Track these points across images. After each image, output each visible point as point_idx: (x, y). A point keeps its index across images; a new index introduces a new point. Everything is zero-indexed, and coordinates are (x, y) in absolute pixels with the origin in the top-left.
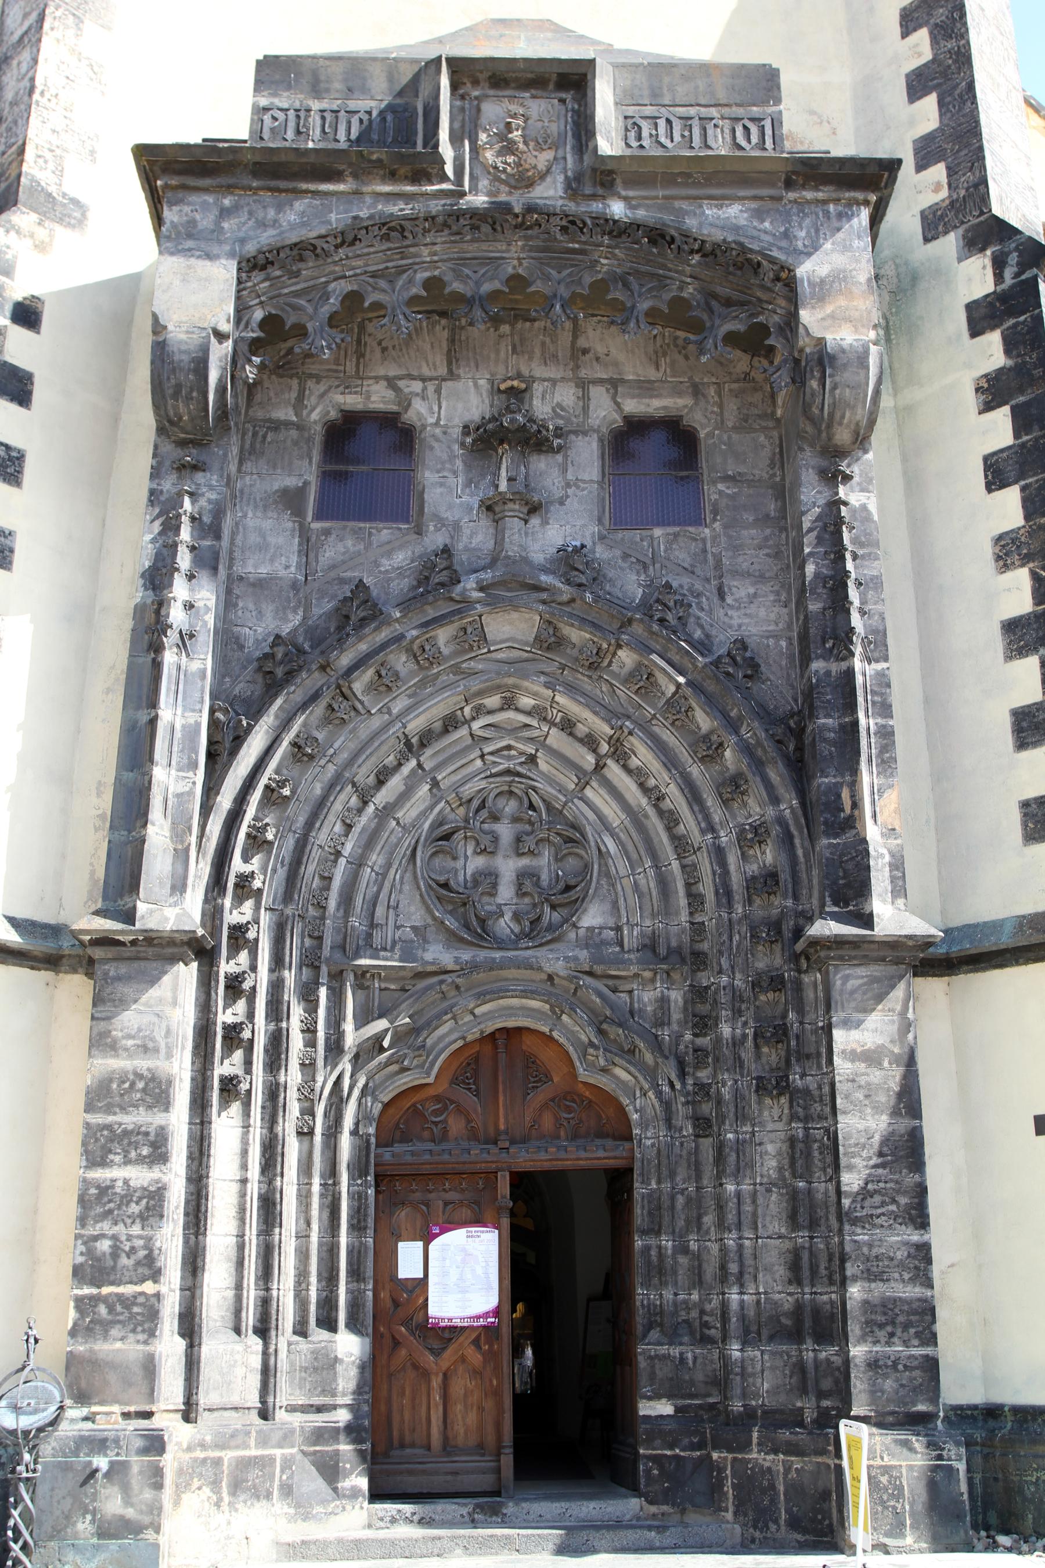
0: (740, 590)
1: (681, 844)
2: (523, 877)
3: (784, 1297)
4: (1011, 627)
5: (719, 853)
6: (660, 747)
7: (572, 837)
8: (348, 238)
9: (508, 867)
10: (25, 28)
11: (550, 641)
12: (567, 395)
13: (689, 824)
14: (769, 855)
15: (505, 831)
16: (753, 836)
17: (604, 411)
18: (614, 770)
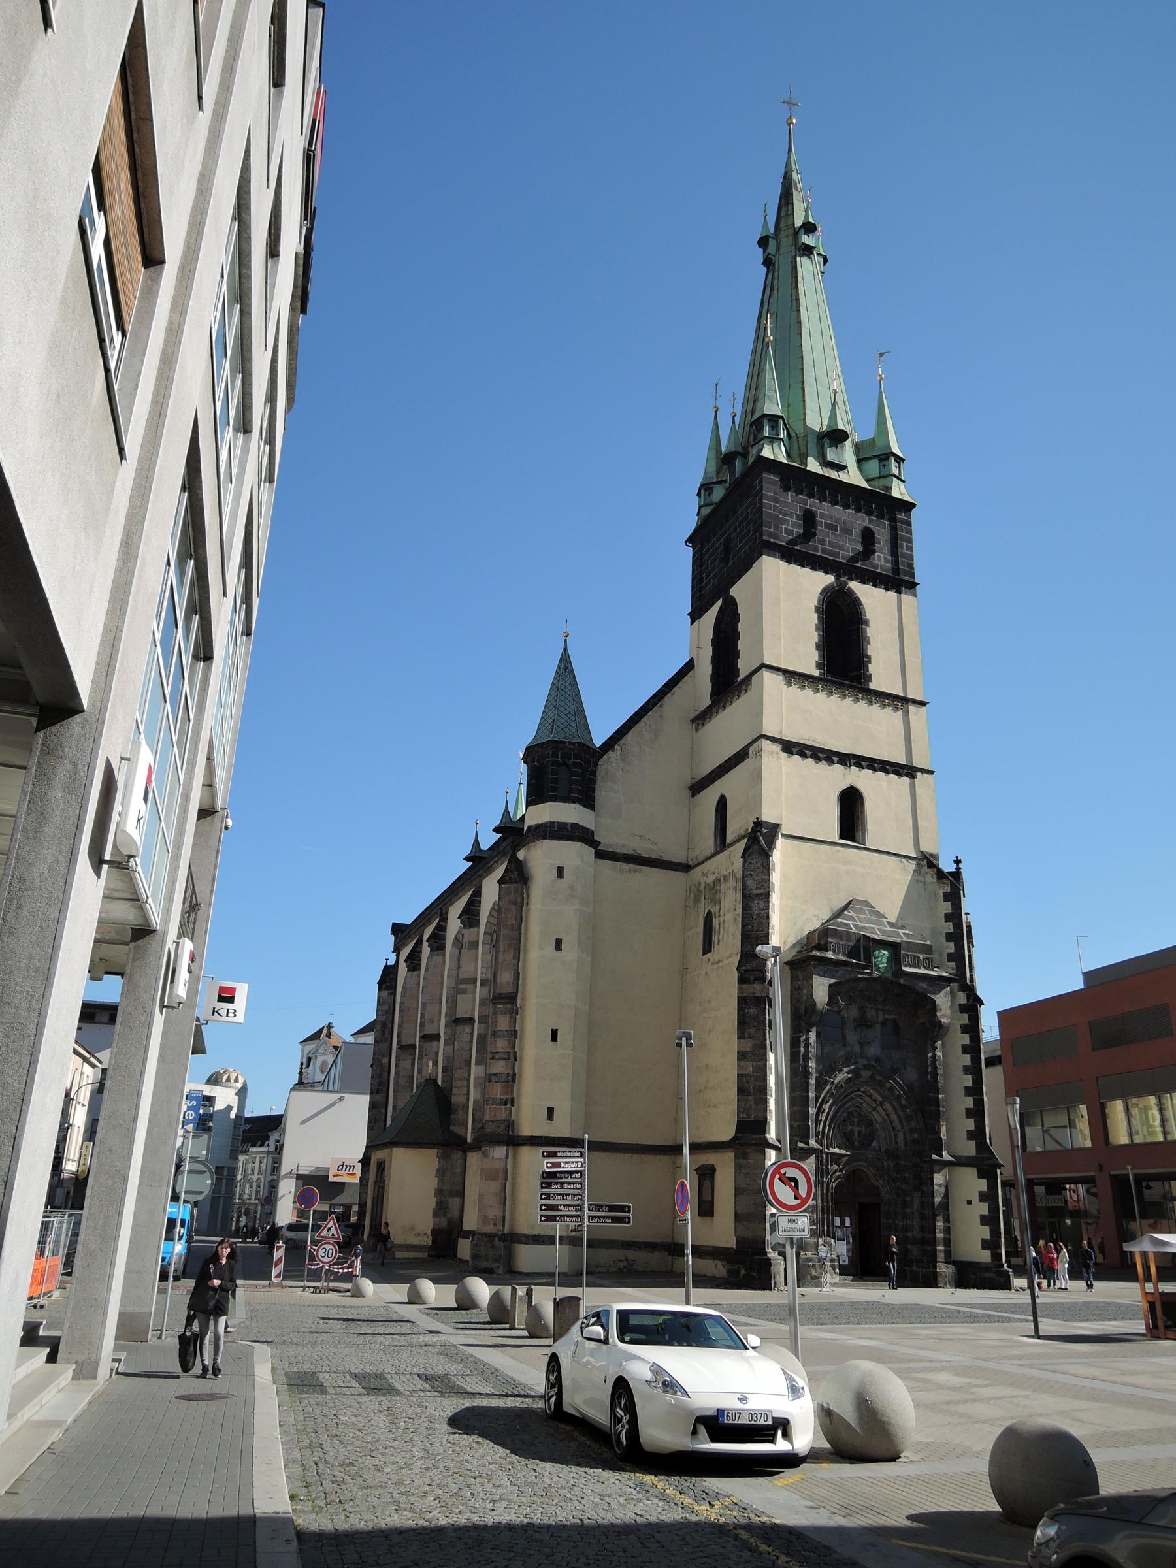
0: (909, 1069)
1: (894, 1128)
2: (860, 1133)
3: (918, 1235)
4: (966, 1088)
5: (905, 1134)
6: (893, 1107)
7: (870, 1123)
8: (848, 981)
9: (856, 1129)
10: (759, 892)
11: (872, 1077)
12: (873, 1012)
13: (898, 1126)
14: (916, 1135)
15: (855, 1120)
16: (912, 1130)
17: (881, 1019)
18: (880, 1109)
